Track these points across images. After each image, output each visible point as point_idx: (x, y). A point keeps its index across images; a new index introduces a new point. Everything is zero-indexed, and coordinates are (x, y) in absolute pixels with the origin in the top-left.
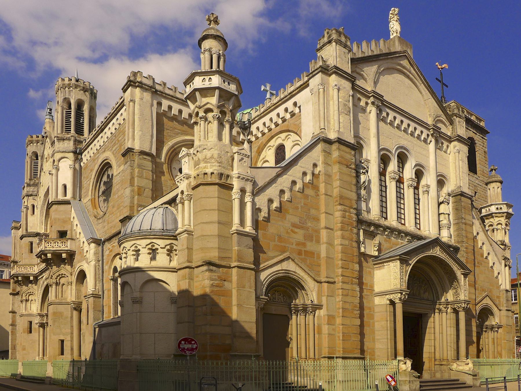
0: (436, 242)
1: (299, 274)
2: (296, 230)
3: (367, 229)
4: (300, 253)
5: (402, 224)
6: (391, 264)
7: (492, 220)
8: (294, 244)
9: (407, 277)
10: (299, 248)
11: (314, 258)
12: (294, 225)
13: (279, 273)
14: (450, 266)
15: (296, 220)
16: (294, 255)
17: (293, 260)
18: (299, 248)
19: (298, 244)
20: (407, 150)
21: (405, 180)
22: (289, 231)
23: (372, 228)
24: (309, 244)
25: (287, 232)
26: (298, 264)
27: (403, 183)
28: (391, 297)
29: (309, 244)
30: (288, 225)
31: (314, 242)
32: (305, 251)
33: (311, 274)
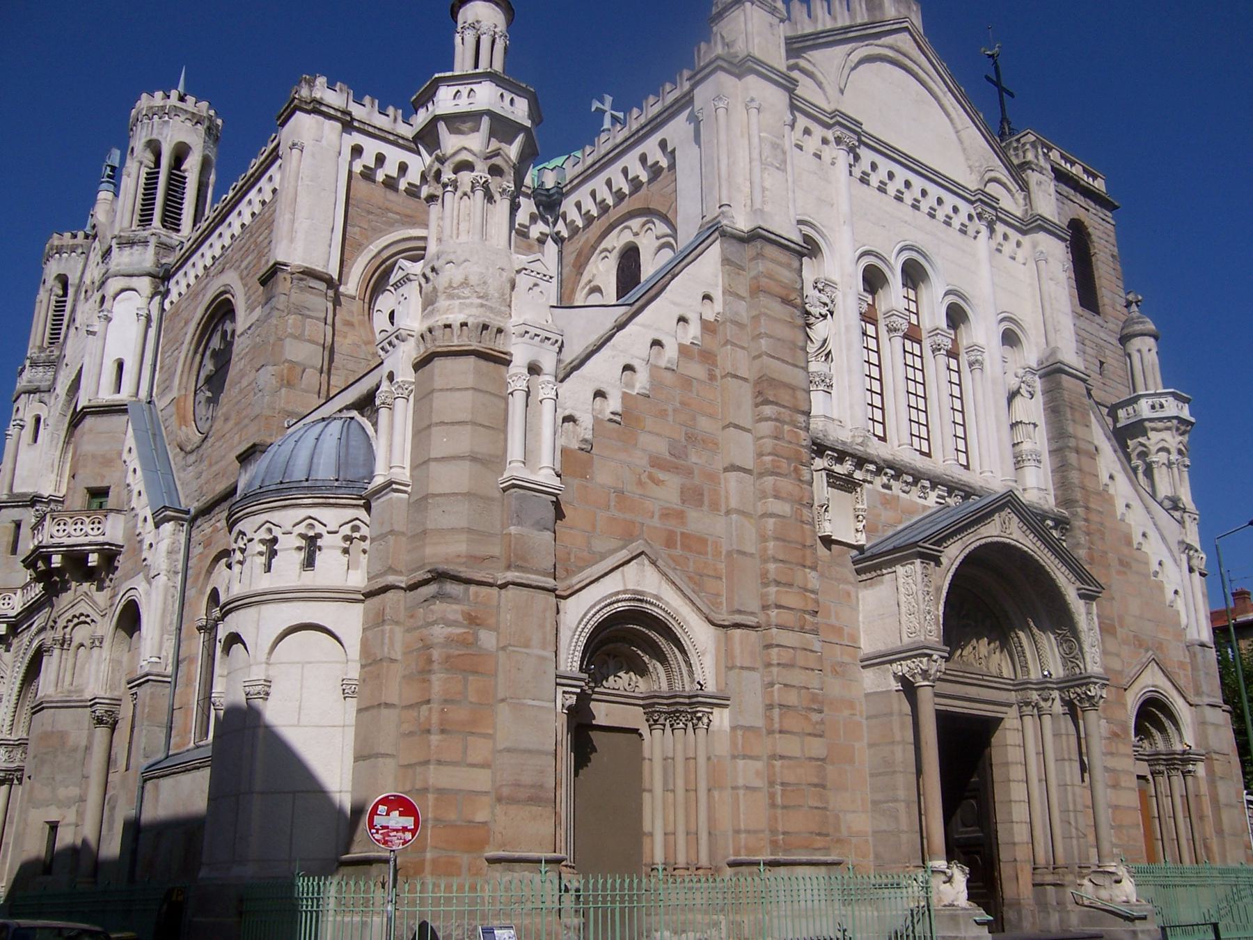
0: (1009, 502)
2: (661, 475)
3: (838, 469)
4: (670, 542)
5: (922, 453)
8: (657, 516)
9: (941, 608)
11: (706, 553)
12: (656, 462)
13: (618, 601)
20: (924, 256)
21: (924, 335)
22: (644, 478)
24: (692, 514)
25: (640, 483)
27: (919, 342)
29: (692, 514)
30: (640, 460)
31: (705, 508)
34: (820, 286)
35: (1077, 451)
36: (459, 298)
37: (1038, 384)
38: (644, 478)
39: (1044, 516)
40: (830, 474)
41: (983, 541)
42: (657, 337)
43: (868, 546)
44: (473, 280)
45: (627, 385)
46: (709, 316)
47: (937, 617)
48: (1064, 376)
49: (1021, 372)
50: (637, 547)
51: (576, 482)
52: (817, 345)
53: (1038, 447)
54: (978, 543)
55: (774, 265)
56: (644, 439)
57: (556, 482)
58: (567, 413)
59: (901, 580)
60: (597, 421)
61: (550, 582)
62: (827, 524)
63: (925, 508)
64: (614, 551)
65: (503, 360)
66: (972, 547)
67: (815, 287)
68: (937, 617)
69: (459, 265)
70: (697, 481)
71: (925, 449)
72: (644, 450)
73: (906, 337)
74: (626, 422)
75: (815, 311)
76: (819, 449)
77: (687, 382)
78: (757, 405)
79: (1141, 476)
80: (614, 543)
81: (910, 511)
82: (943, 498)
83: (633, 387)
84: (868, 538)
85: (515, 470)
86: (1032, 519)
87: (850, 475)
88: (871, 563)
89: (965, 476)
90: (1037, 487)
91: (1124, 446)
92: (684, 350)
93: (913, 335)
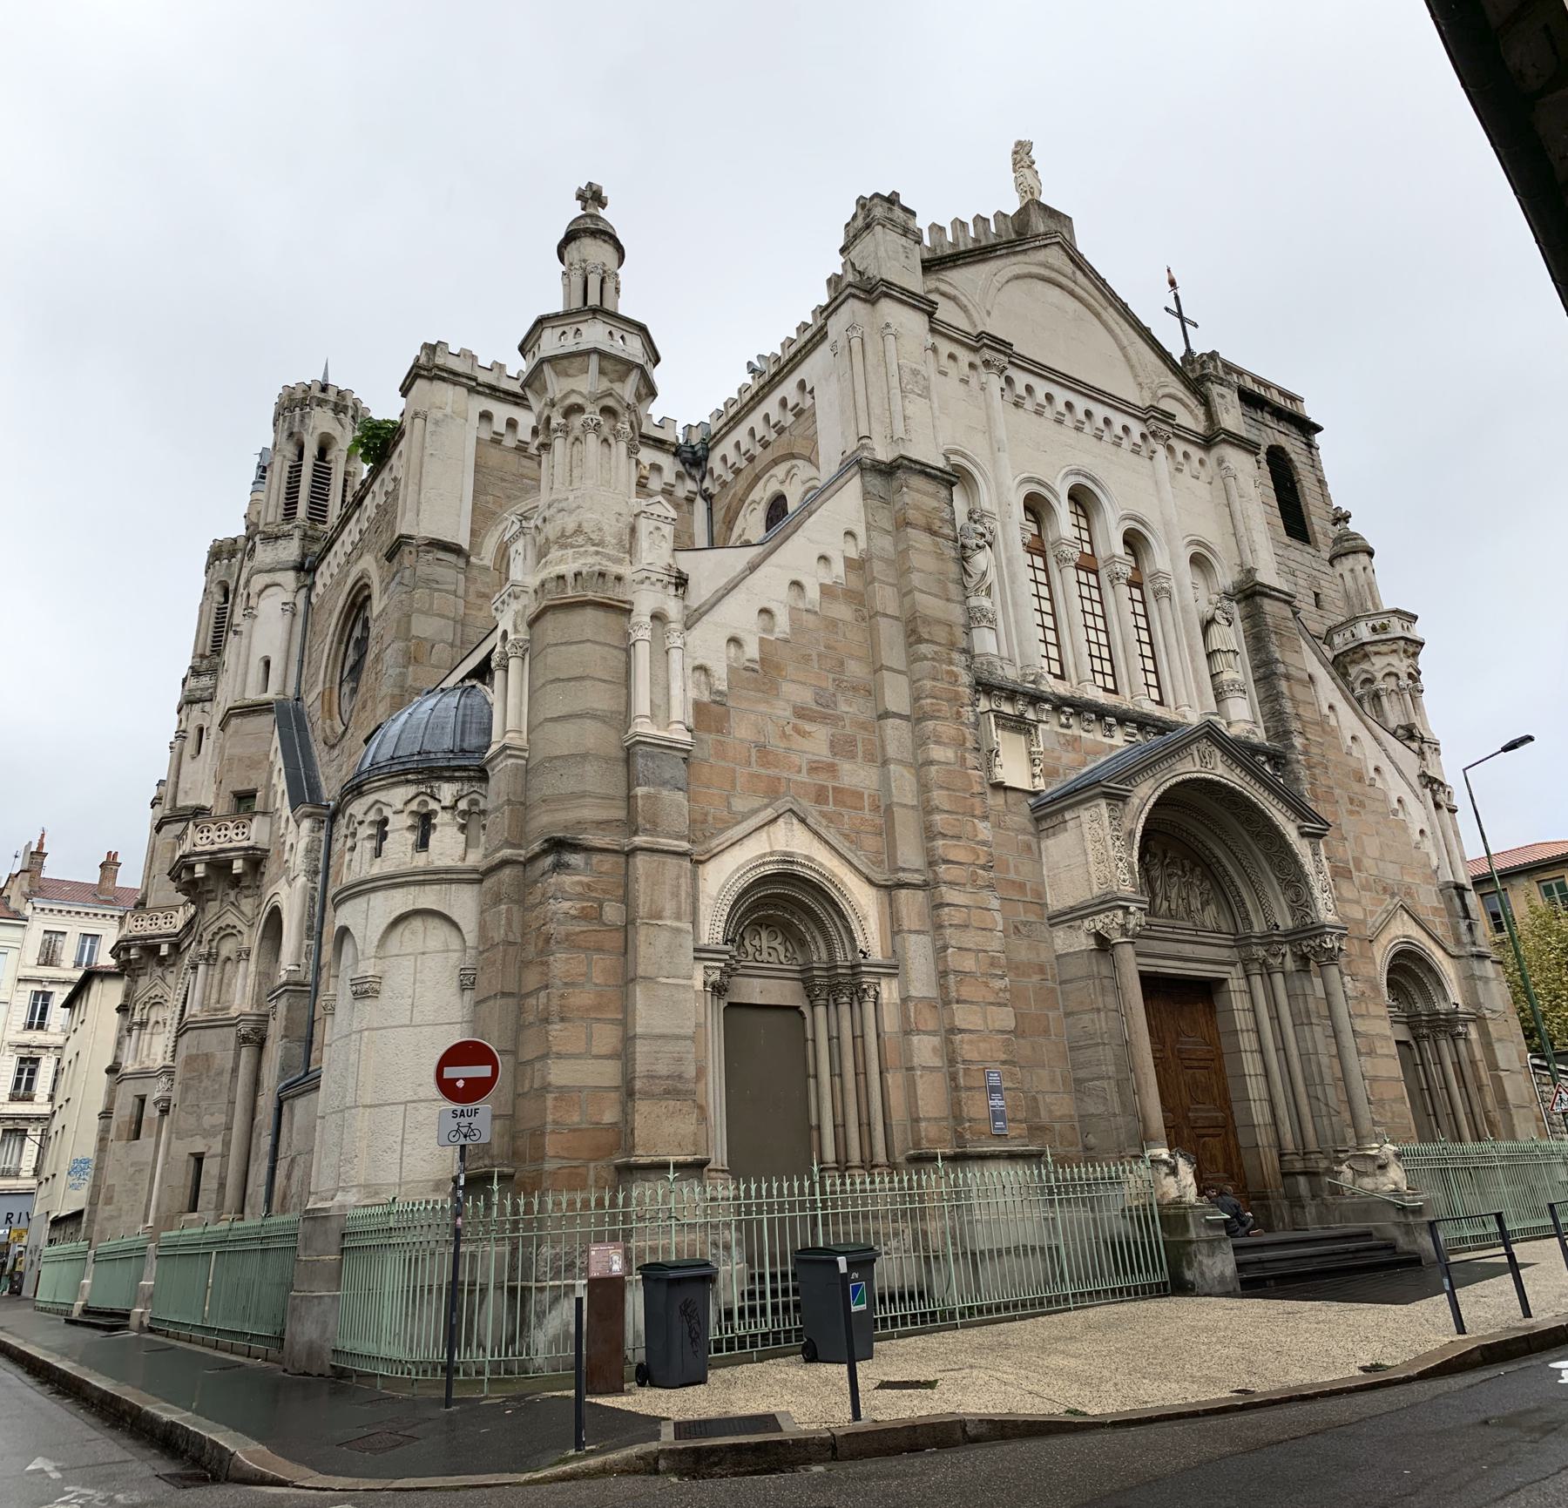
0: (1210, 733)
1: (821, 865)
2: (808, 727)
3: (1007, 708)
4: (820, 796)
5: (1105, 689)
6: (1085, 814)
7: (1365, 666)
9: (1136, 854)
10: (822, 779)
11: (862, 809)
12: (801, 713)
13: (764, 864)
14: (1262, 812)
15: (805, 696)
16: (806, 803)
17: (803, 821)
18: (822, 779)
19: (814, 769)
21: (1100, 564)
22: (789, 730)
23: (1020, 706)
25: (784, 735)
26: (816, 833)
27: (1096, 573)
28: (1098, 923)
29: (845, 766)
30: (783, 711)
31: (859, 760)
32: (834, 788)
33: (855, 861)
34: (975, 517)
35: (1288, 677)
36: (572, 547)
37: (1236, 610)
38: (789, 730)
39: (1255, 750)
40: (999, 715)
41: (1180, 778)
42: (798, 578)
43: (1048, 791)
44: (587, 528)
45: (764, 631)
46: (854, 554)
47: (1131, 865)
48: (1266, 601)
49: (1215, 598)
50: (783, 804)
51: (710, 738)
52: (976, 578)
53: (1240, 677)
54: (1174, 781)
55: (918, 495)
56: (787, 688)
57: (688, 738)
58: (697, 663)
59: (1086, 827)
60: (730, 668)
61: (685, 845)
62: (997, 770)
63: (1112, 747)
64: (755, 812)
65: (623, 610)
66: (1168, 784)
67: (970, 518)
68: (1131, 865)
69: (571, 512)
70: (848, 731)
71: (1110, 686)
72: (788, 701)
73: (1078, 567)
74: (764, 673)
75: (972, 542)
76: (984, 687)
77: (832, 624)
78: (911, 645)
79: (1366, 706)
80: (757, 802)
81: (1097, 750)
82: (1133, 735)
83: (771, 631)
84: (1048, 784)
85: (644, 727)
86: (1239, 752)
87: (1022, 715)
88: (1048, 811)
89: (1158, 711)
90: (1243, 717)
91: (1345, 675)
92: (826, 590)
93: (1088, 565)
